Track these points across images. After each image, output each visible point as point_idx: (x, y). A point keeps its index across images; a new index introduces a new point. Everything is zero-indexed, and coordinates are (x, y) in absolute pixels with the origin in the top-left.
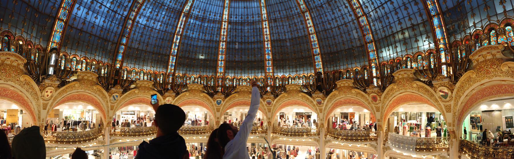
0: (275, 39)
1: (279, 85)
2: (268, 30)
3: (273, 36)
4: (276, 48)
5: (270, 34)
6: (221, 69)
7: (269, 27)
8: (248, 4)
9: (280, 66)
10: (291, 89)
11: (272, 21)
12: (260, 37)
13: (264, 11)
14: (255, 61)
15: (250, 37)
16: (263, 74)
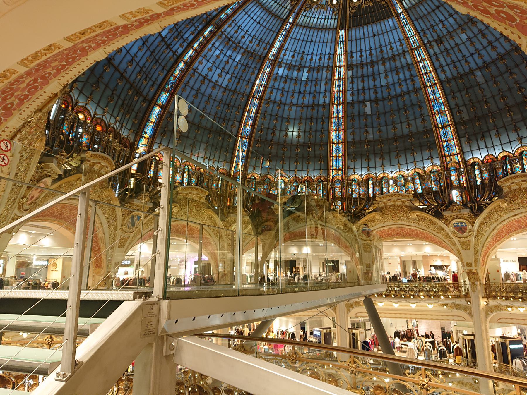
0: (449, 75)
1: (482, 181)
2: (427, 63)
3: (444, 71)
4: (458, 95)
5: (435, 70)
6: (337, 162)
7: (430, 57)
8: (376, 28)
9: (475, 134)
10: (514, 187)
11: (434, 43)
12: (413, 80)
13: (411, 32)
14: (411, 135)
15: (392, 87)
16: (437, 162)
